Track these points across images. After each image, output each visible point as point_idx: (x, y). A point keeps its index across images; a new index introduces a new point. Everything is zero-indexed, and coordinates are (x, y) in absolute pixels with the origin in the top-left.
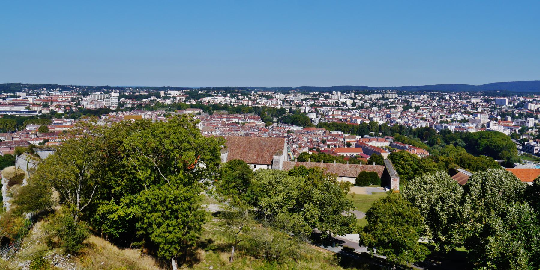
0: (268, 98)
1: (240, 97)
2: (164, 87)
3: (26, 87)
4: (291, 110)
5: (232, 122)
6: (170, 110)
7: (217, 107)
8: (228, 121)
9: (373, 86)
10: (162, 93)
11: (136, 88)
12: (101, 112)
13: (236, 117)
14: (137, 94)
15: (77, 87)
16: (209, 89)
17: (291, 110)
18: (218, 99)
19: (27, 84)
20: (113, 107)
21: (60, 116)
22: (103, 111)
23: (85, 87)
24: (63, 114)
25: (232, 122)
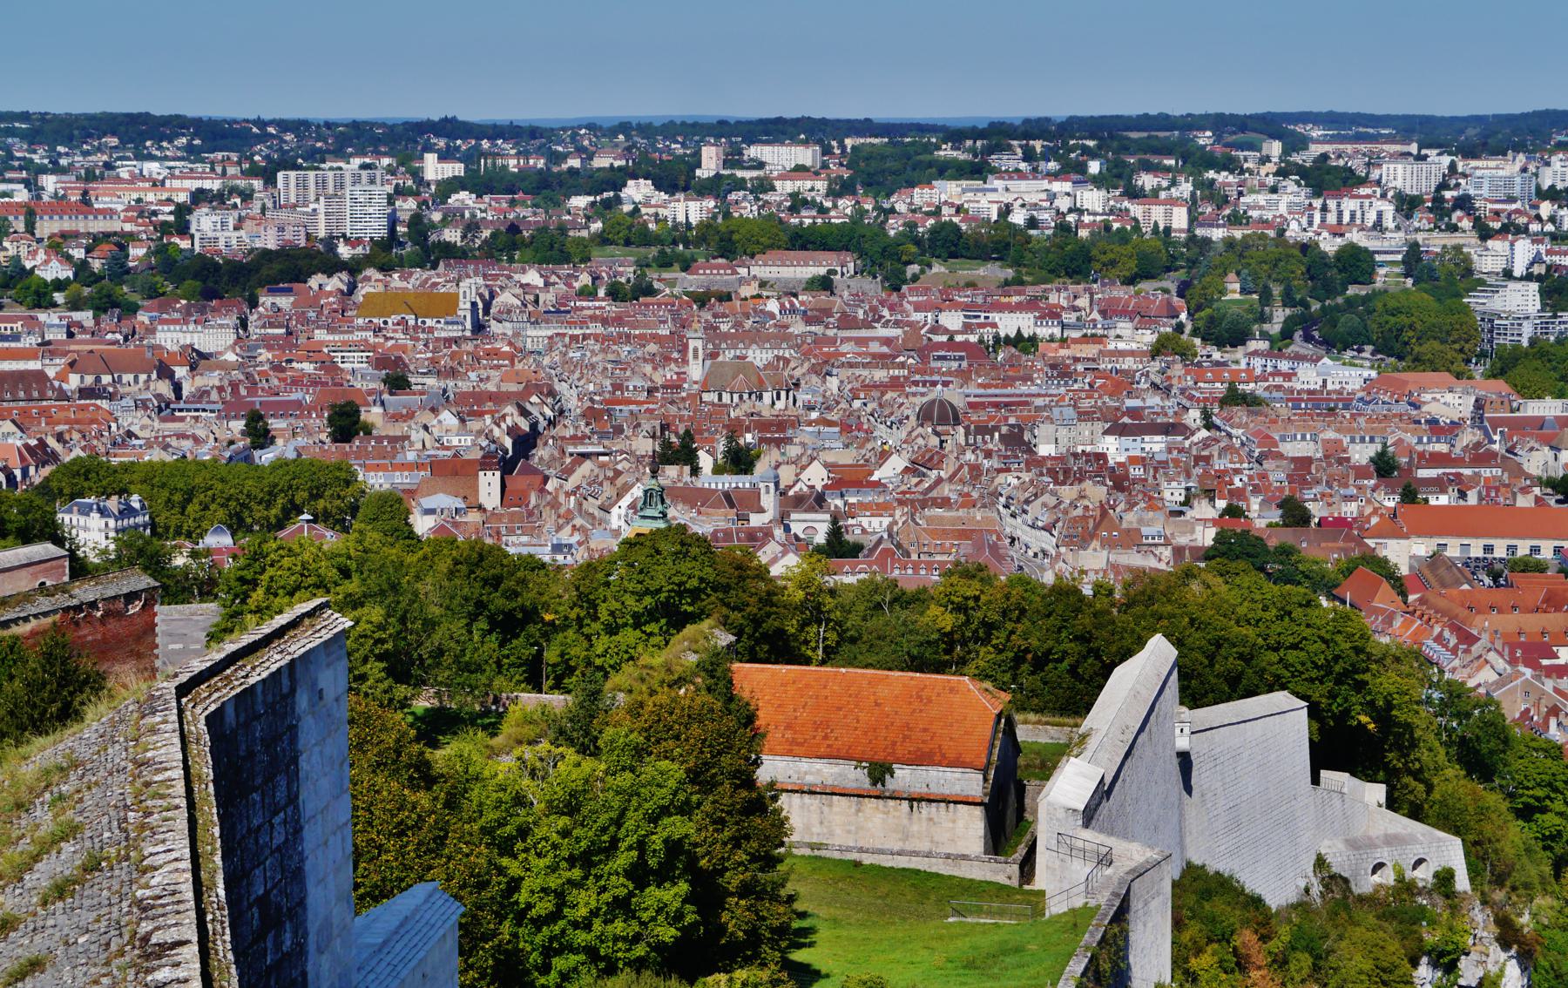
0: (1326, 180)
2: (779, 121)
3: (11, 132)
4: (1413, 258)
5: (988, 335)
6: (665, 263)
7: (950, 243)
10: (710, 162)
11: (612, 132)
12: (264, 272)
13: (1030, 305)
14: (575, 163)
15: (284, 125)
16: (997, 135)
17: (1413, 258)
18: (1020, 195)
19: (25, 116)
21: (41, 297)
22: (277, 266)
23: (328, 125)
24: (59, 285)
25: (988, 335)
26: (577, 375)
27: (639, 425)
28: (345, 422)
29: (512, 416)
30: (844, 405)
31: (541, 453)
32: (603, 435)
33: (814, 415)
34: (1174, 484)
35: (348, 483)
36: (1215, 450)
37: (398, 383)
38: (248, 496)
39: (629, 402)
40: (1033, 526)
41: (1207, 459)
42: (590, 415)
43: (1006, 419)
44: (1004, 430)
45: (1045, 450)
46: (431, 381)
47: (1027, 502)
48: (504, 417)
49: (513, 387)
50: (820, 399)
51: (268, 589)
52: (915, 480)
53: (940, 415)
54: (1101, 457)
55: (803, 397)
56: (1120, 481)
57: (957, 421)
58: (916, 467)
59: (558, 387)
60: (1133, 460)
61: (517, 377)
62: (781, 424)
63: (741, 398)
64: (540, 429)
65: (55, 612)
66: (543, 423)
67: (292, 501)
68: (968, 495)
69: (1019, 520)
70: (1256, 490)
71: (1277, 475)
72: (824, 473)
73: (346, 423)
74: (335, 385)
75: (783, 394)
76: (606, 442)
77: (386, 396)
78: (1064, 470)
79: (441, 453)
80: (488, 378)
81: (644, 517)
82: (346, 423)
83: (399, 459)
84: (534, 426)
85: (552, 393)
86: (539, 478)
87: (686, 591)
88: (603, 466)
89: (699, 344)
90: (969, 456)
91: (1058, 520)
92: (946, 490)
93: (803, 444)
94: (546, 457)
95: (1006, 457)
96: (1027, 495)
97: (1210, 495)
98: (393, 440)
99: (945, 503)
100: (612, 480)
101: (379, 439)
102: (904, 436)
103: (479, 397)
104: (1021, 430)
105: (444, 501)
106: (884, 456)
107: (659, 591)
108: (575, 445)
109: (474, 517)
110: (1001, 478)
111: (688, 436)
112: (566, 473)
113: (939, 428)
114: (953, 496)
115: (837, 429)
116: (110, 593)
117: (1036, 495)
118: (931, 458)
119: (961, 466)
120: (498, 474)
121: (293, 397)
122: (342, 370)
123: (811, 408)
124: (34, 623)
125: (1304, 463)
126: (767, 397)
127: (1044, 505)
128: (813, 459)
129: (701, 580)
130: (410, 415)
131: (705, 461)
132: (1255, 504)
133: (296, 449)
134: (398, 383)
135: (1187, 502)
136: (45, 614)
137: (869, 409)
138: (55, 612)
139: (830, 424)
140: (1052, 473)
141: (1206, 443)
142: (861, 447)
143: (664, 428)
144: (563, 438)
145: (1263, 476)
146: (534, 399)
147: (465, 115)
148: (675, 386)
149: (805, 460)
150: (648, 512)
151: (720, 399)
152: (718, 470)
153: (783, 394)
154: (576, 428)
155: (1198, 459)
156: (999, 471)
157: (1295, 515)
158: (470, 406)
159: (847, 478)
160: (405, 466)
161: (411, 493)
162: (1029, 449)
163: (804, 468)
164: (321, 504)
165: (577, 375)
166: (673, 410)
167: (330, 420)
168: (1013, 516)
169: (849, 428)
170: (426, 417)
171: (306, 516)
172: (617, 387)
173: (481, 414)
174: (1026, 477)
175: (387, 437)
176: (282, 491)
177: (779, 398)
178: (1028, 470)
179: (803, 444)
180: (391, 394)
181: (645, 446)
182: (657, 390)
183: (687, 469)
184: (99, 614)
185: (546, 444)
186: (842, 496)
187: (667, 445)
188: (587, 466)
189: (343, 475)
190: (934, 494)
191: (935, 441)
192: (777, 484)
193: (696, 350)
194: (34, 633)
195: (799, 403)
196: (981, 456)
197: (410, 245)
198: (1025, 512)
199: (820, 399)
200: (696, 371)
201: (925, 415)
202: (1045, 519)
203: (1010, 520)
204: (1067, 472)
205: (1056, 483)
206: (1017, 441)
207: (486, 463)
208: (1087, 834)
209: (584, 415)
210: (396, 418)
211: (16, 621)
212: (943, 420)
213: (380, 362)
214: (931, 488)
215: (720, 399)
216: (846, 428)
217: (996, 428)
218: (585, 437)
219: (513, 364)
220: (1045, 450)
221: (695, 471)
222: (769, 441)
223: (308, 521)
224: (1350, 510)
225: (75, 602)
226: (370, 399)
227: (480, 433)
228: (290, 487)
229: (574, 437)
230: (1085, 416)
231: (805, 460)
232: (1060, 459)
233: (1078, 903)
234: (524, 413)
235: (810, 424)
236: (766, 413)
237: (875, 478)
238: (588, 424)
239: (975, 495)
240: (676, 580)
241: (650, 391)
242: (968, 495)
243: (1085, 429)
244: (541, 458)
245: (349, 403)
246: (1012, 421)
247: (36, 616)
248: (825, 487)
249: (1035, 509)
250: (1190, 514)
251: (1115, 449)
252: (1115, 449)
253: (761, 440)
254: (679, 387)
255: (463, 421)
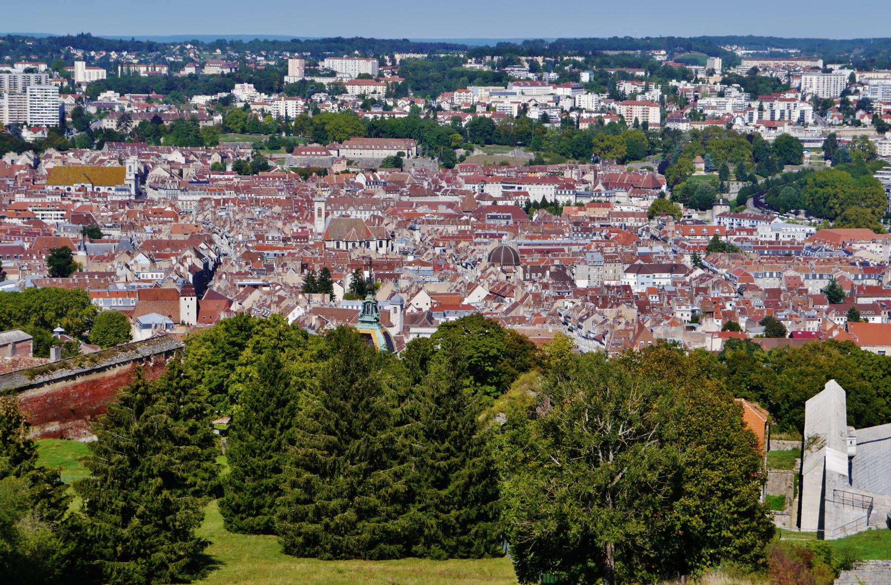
0: (758, 87)
1: (627, 87)
2: (338, 40)
4: (831, 145)
6: (275, 146)
7: (486, 132)
8: (506, 196)
9: (791, 37)
10: (295, 71)
11: (212, 47)
13: (552, 179)
14: (189, 70)
16: (508, 53)
17: (831, 145)
18: (530, 97)
20: (36, 129)
25: (522, 200)
26: (227, 228)
27: (285, 264)
28: (62, 262)
29: (192, 260)
30: (430, 251)
31: (216, 285)
32: (260, 273)
33: (410, 258)
34: (683, 308)
35: (84, 305)
36: (710, 283)
37: (94, 234)
38: (9, 315)
39: (272, 248)
40: (586, 338)
41: (705, 290)
42: (248, 257)
43: (553, 261)
44: (553, 269)
45: (581, 284)
46: (116, 233)
47: (581, 320)
48: (185, 258)
49: (181, 237)
50: (412, 247)
51: (254, 348)
52: (495, 305)
53: (505, 258)
54: (627, 288)
55: (398, 245)
56: (643, 307)
57: (518, 263)
58: (497, 295)
59: (216, 237)
60: (651, 291)
61: (183, 229)
62: (391, 265)
63: (354, 245)
64: (211, 268)
65: (128, 362)
66: (211, 265)
67: (42, 319)
68: (538, 314)
69: (575, 333)
70: (743, 312)
71: (757, 302)
72: (428, 299)
73: (62, 263)
74: (45, 234)
75: (384, 243)
76: (263, 277)
77: (87, 243)
78: (603, 297)
79: (142, 284)
80: (160, 231)
81: (363, 322)
82: (62, 263)
83: (111, 288)
84: (206, 265)
85: (211, 242)
86: (224, 302)
87: (489, 357)
88: (268, 293)
89: (322, 205)
90: (530, 287)
91: (606, 333)
92: (521, 311)
93: (410, 279)
94: (222, 288)
95: (559, 288)
96: (580, 315)
97: (710, 314)
98: (102, 275)
99: (522, 320)
100: (278, 303)
101: (91, 275)
102: (479, 274)
103: (160, 244)
104: (564, 269)
105: (155, 318)
106: (471, 287)
107: (471, 357)
108: (242, 280)
109: (180, 330)
110: (559, 303)
111: (326, 272)
112: (242, 298)
113: (505, 268)
114: (528, 316)
115: (431, 268)
116: (157, 351)
117: (588, 315)
118: (504, 289)
119: (527, 295)
120: (195, 299)
121: (17, 243)
122: (46, 224)
123: (405, 253)
124: (118, 368)
125: (774, 293)
126: (373, 245)
127: (594, 322)
128: (419, 290)
129: (498, 350)
130: (111, 258)
131: (339, 291)
132: (742, 322)
133: (32, 281)
134: (94, 234)
135: (695, 319)
136: (124, 363)
137: (449, 252)
138: (128, 362)
139: (424, 264)
140: (594, 300)
141: (702, 279)
142: (453, 280)
143: (303, 267)
144: (231, 274)
145: (747, 302)
146: (202, 245)
147: (97, 32)
148: (302, 237)
149: (413, 290)
150: (366, 318)
151: (338, 246)
152: (347, 297)
153: (384, 243)
154: (241, 266)
155: (698, 290)
156: (556, 298)
157: (774, 329)
158: (157, 250)
159: (444, 303)
160: (118, 294)
161: (130, 313)
162: (572, 282)
163: (413, 296)
164: (65, 320)
165: (227, 228)
166: (308, 254)
167: (50, 261)
168: (571, 330)
169: (438, 266)
170: (126, 258)
171: (59, 329)
172: (259, 237)
173: (166, 257)
174: (579, 302)
175: (97, 273)
176: (35, 311)
177: (381, 246)
178: (577, 298)
179: (410, 279)
180: (91, 242)
181: (296, 279)
182: (289, 239)
183: (327, 296)
184: (151, 364)
185: (220, 278)
186: (445, 315)
187: (309, 279)
188: (256, 294)
189: (81, 299)
190: (513, 314)
191: (503, 277)
192: (402, 306)
193: (320, 210)
194: (118, 376)
195: (396, 249)
196: (540, 287)
197: (75, 130)
198: (580, 327)
199: (412, 247)
200: (320, 226)
201: (494, 258)
202: (596, 331)
203: (569, 333)
204: (604, 299)
205: (597, 305)
206: (563, 277)
207: (186, 291)
208: (852, 490)
209: (243, 256)
210: (101, 259)
211: (108, 367)
212: (507, 262)
213: (76, 218)
214: (509, 310)
215: (338, 246)
216: (437, 268)
217: (546, 268)
218: (246, 273)
219: (176, 220)
220: (581, 284)
221: (332, 297)
222: (383, 277)
223: (61, 333)
224: (813, 326)
225: (139, 356)
226: (76, 245)
227: (171, 269)
228: (41, 308)
229: (239, 273)
230: (609, 259)
231: (413, 290)
232: (596, 289)
233: (864, 528)
234: (199, 256)
235: (410, 264)
236: (374, 257)
237: (465, 302)
238: (247, 264)
239: (544, 315)
240: (483, 349)
241: (285, 240)
242: (538, 314)
243: (610, 269)
244: (219, 288)
245: (65, 248)
246: (557, 262)
247: (119, 364)
248: (432, 308)
249: (587, 325)
250: (699, 329)
251: (636, 283)
252: (636, 283)
253: (378, 276)
254: (307, 238)
255: (153, 261)
